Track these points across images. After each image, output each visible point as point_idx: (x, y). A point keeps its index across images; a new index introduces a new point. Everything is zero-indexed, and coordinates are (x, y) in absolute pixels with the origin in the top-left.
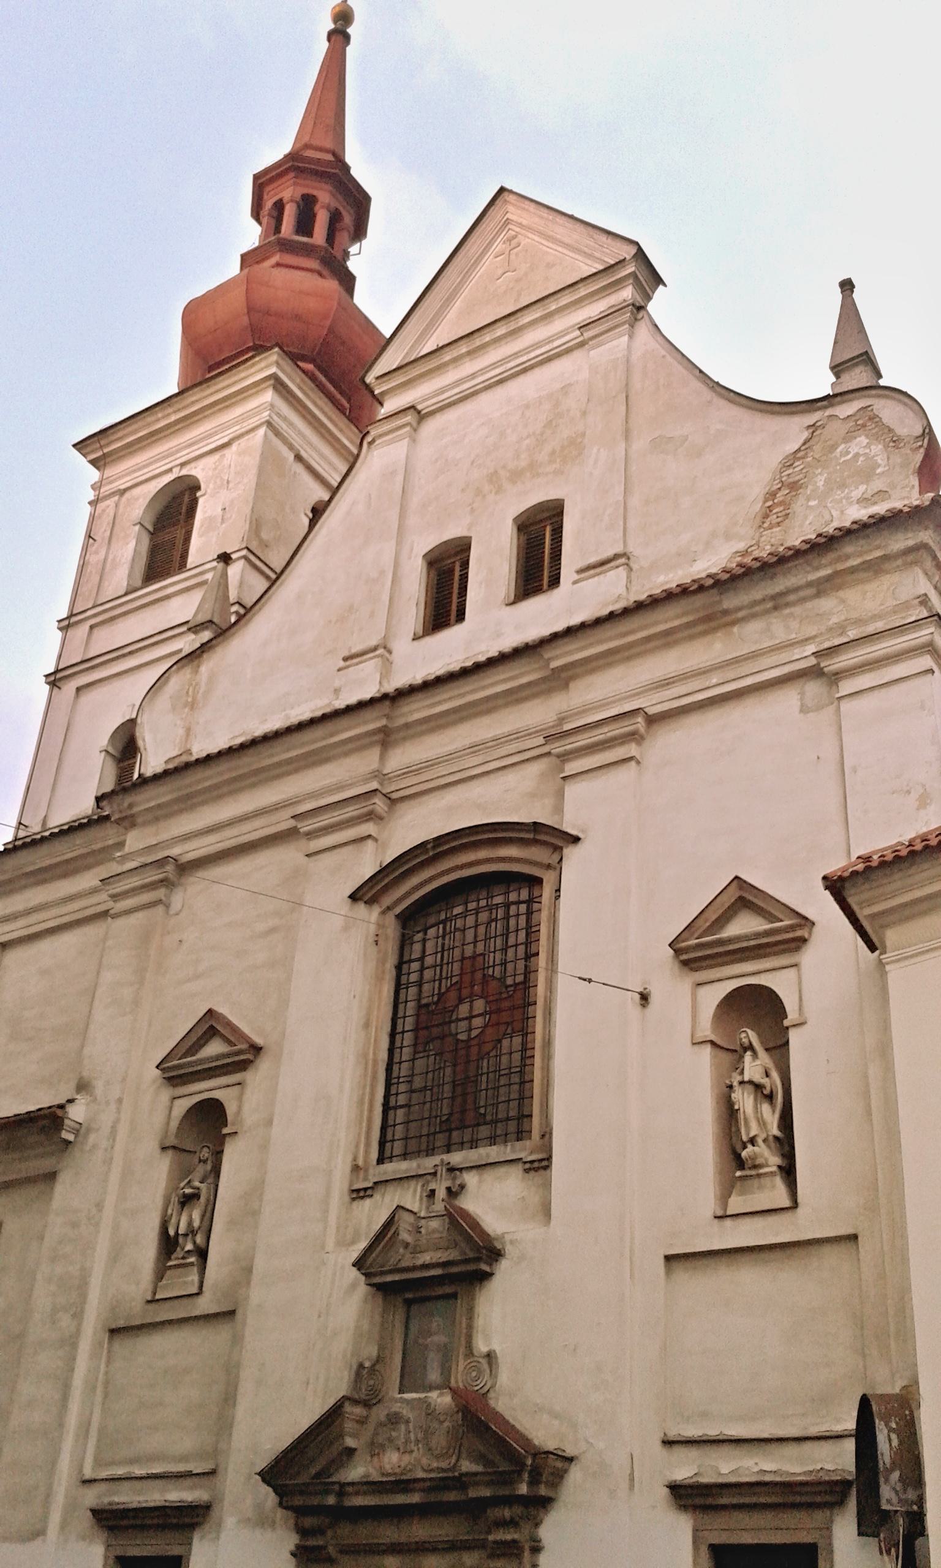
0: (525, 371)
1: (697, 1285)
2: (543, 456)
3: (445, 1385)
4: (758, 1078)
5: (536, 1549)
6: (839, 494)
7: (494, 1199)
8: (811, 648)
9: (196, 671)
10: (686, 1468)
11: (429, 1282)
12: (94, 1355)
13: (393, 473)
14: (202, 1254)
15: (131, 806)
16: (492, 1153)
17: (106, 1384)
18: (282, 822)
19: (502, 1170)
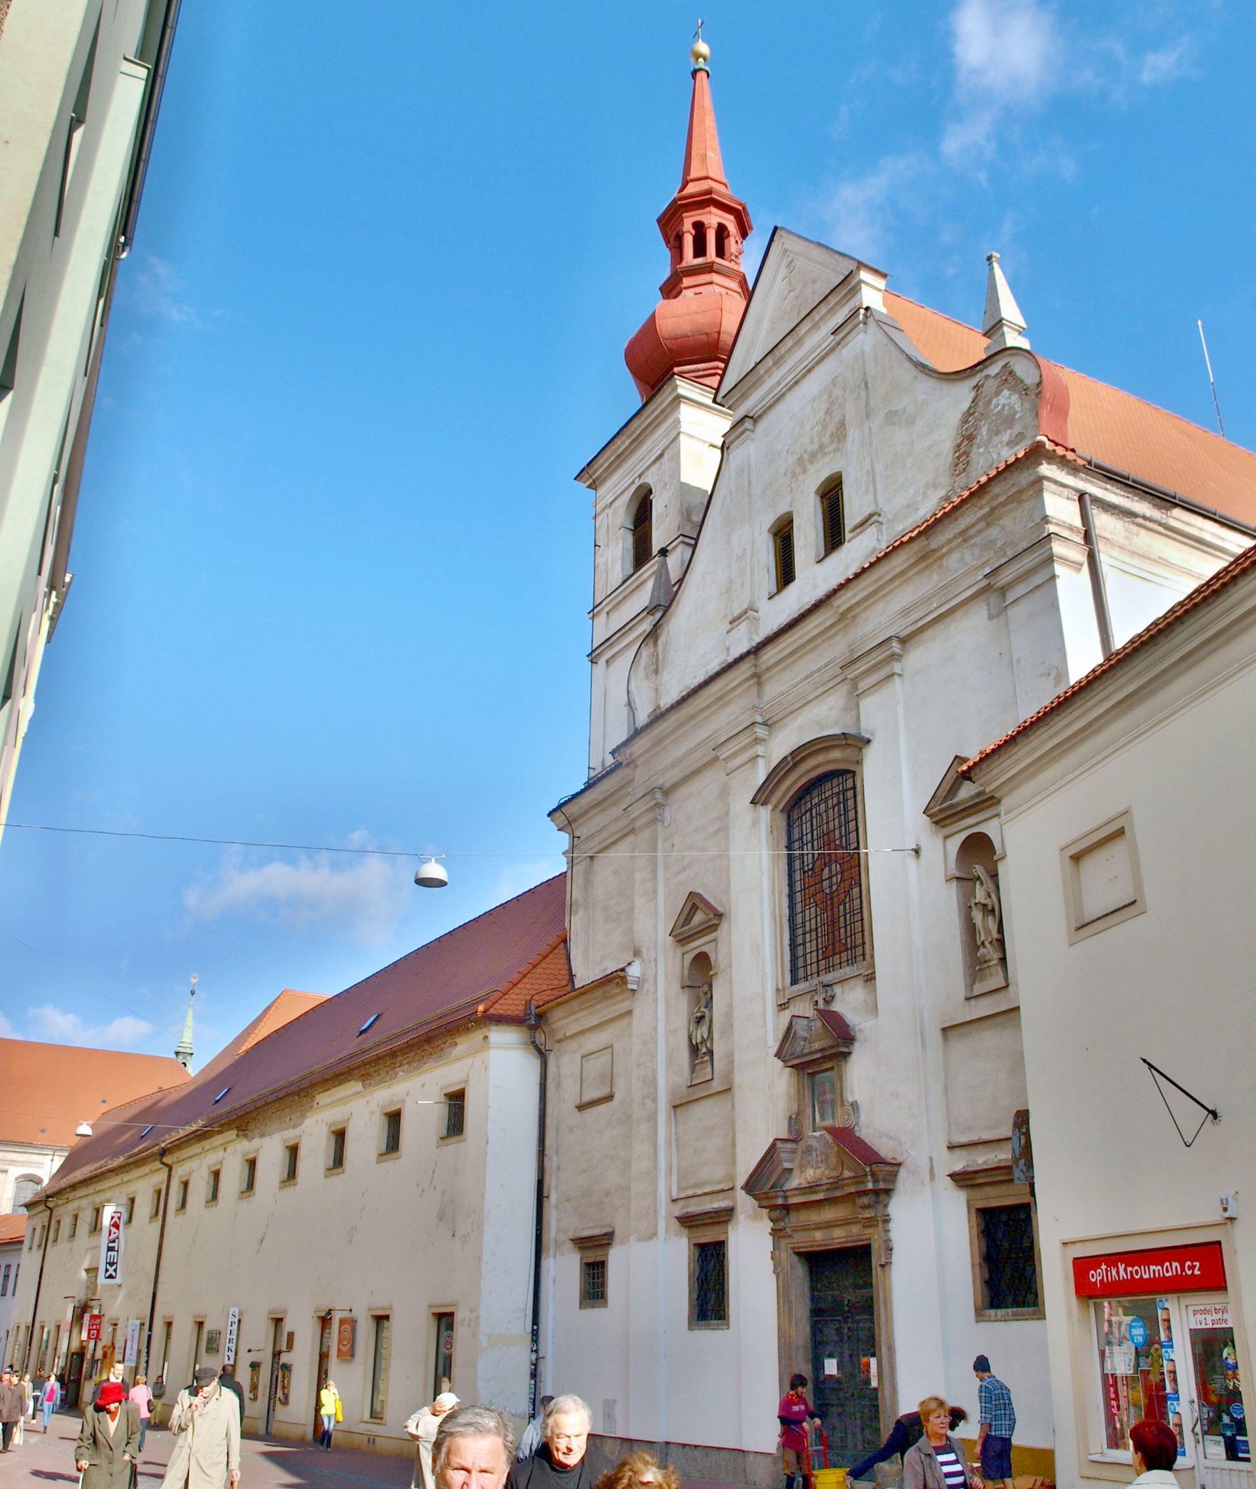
0: (809, 371)
1: (961, 1047)
2: (826, 440)
4: (983, 901)
5: (887, 1221)
6: (996, 439)
7: (849, 1002)
10: (960, 1163)
12: (668, 1123)
14: (710, 1052)
16: (847, 971)
19: (853, 982)
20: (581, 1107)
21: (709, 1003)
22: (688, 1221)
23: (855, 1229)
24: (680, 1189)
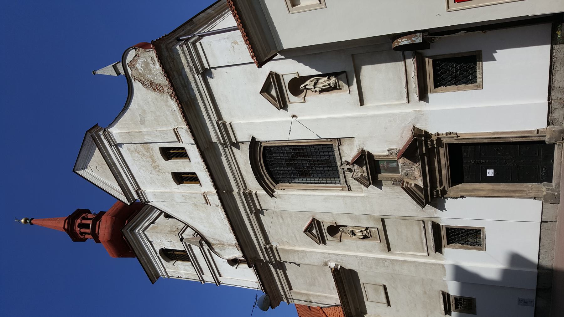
2: (148, 154)
3: (397, 162)
5: (438, 134)
7: (349, 153)
8: (196, 76)
9: (213, 244)
10: (415, 96)
11: (372, 168)
13: (155, 195)
14: (367, 229)
16: (337, 153)
18: (253, 217)
20: (389, 304)
22: (438, 248)
23: (442, 151)
24: (423, 252)
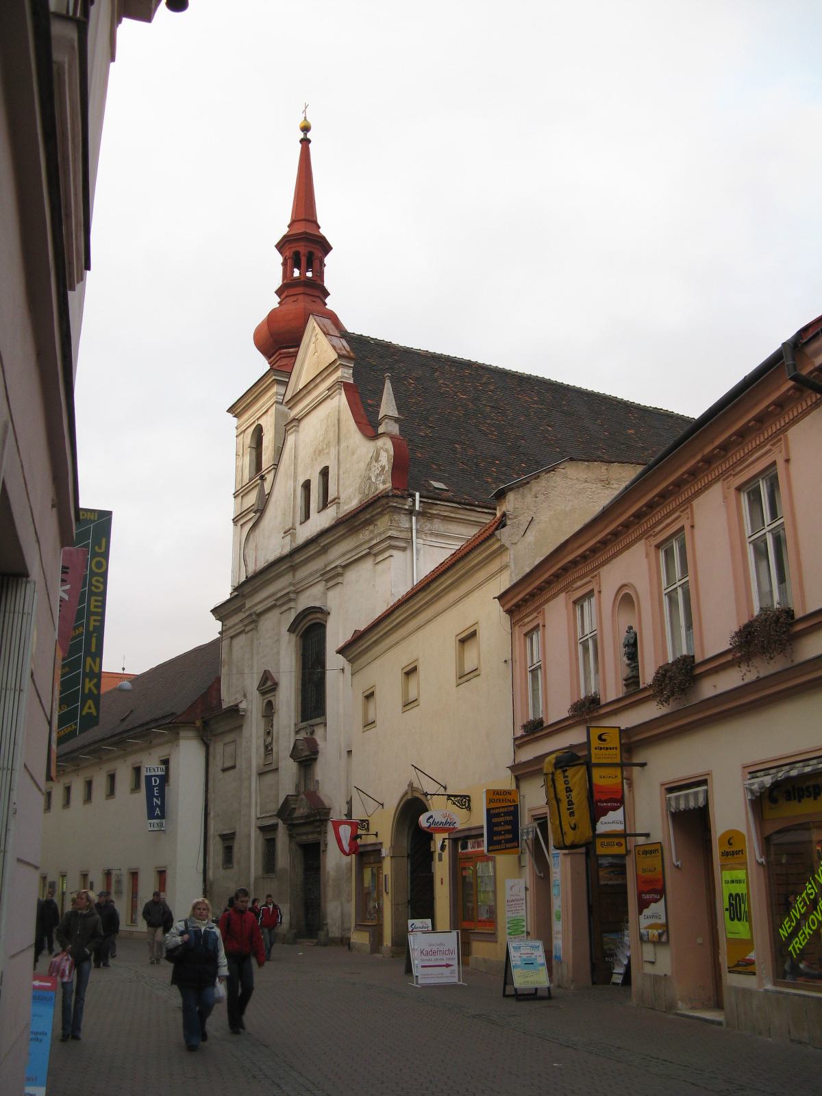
11: (306, 757)
15: (243, 592)
17: (260, 790)
20: (224, 770)
21: (272, 726)
